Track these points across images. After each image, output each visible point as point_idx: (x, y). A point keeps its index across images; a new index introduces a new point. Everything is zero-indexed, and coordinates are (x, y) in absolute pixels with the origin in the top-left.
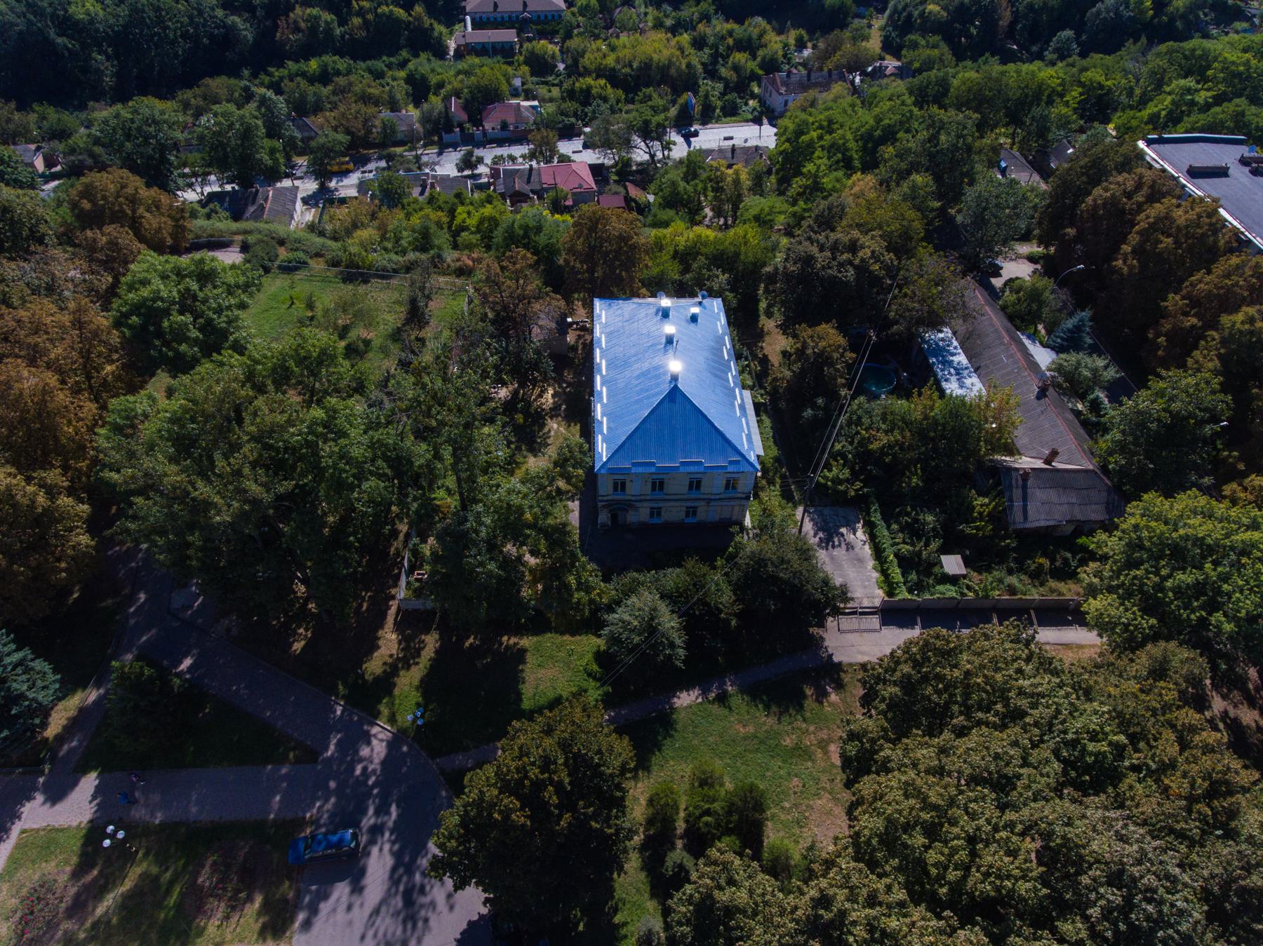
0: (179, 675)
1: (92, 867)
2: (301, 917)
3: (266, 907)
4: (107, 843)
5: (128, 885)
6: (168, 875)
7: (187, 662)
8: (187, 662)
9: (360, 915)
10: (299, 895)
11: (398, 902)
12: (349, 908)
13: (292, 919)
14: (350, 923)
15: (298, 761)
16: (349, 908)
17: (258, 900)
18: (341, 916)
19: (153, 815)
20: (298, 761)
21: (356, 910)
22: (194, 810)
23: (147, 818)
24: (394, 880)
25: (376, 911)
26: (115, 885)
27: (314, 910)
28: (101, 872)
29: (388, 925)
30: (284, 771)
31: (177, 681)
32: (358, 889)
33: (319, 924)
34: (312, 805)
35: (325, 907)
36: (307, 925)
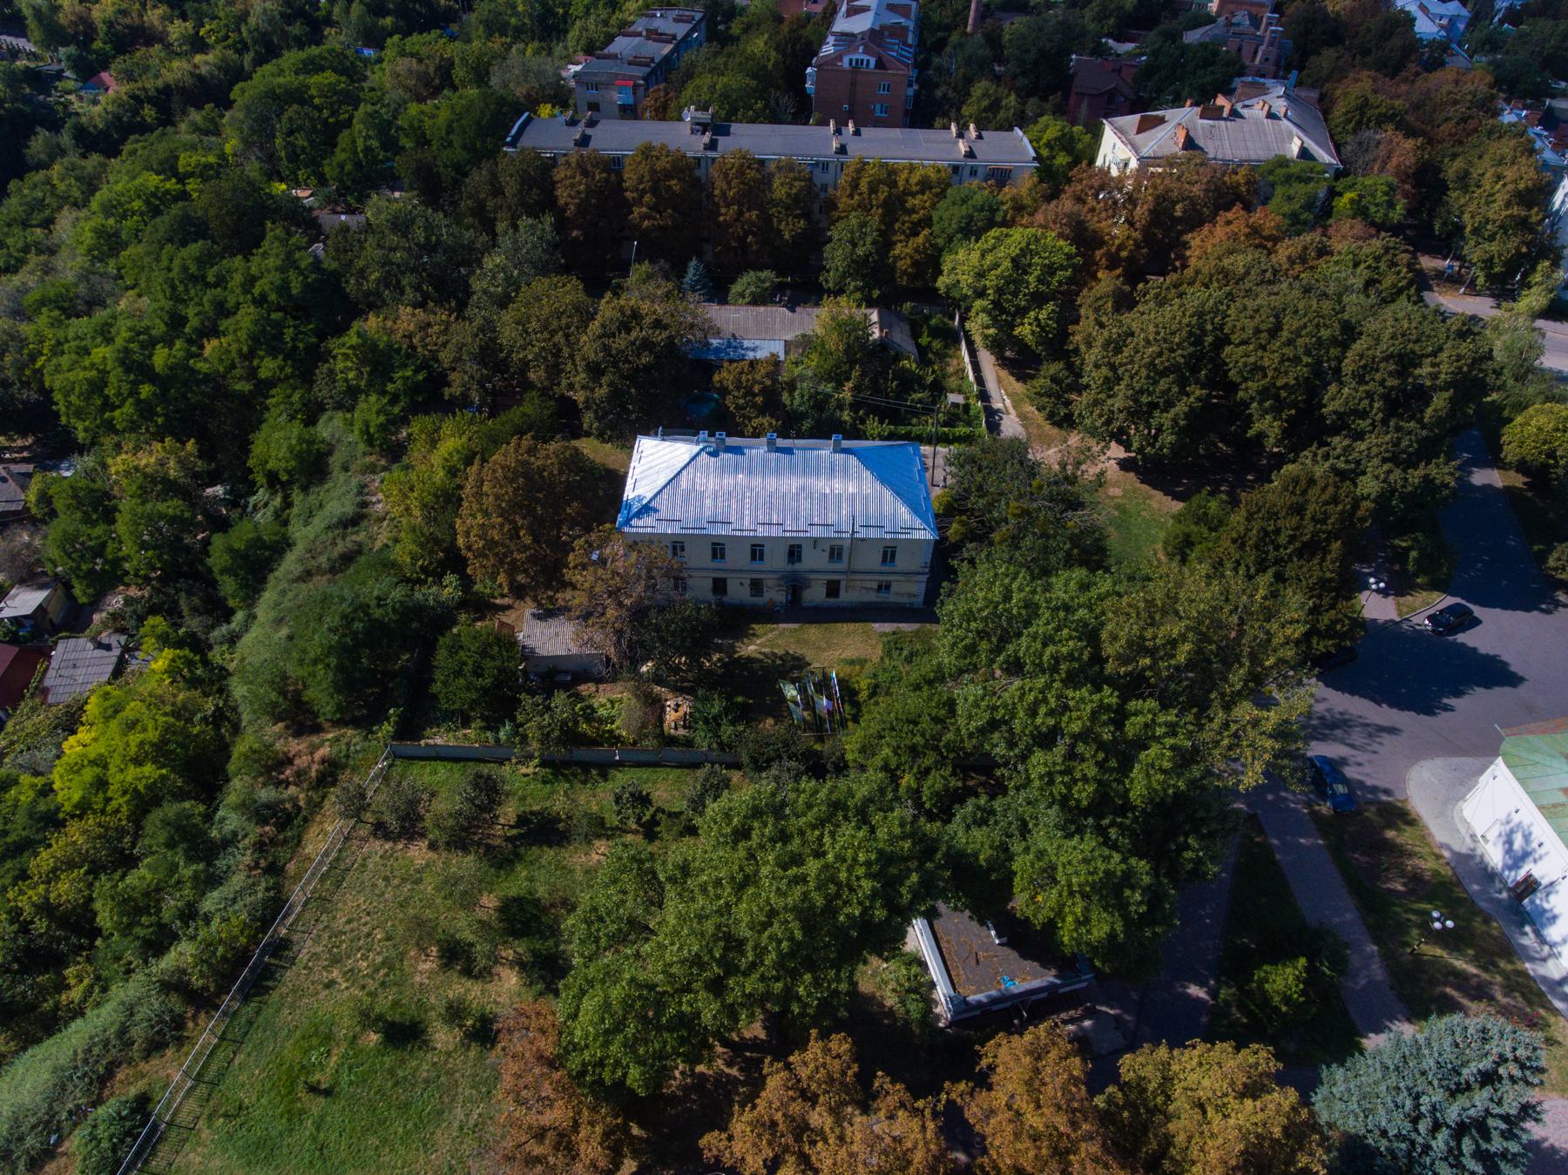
0: (1214, 994)
1: (1445, 996)
2: (1384, 798)
3: (1391, 826)
4: (1449, 924)
5: (1439, 952)
6: (1413, 917)
7: (1195, 991)
8: (1195, 991)
9: (1361, 757)
10: (1371, 802)
11: (1338, 732)
12: (1360, 764)
13: (1389, 803)
14: (1370, 762)
15: (1261, 831)
16: (1360, 764)
17: (1390, 834)
18: (1367, 769)
19: (1372, 956)
20: (1261, 831)
21: (1359, 759)
22: (1348, 916)
23: (1376, 959)
24: (1324, 739)
25: (1352, 746)
26: (1447, 965)
27: (1374, 789)
28: (1445, 984)
29: (1357, 737)
30: (1275, 842)
31: (1224, 993)
32: (1343, 761)
33: (1382, 784)
34: (1294, 810)
35: (1369, 782)
36: (1387, 792)
